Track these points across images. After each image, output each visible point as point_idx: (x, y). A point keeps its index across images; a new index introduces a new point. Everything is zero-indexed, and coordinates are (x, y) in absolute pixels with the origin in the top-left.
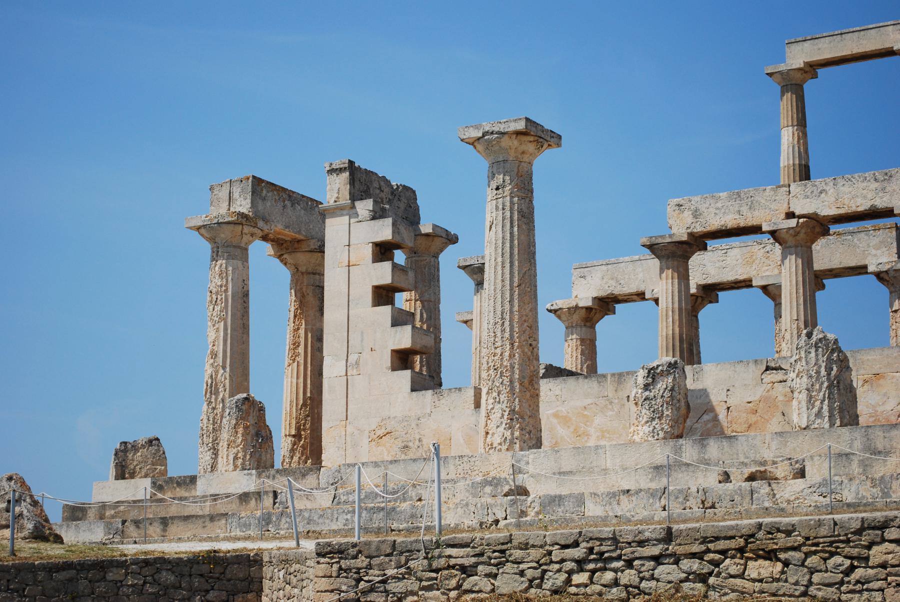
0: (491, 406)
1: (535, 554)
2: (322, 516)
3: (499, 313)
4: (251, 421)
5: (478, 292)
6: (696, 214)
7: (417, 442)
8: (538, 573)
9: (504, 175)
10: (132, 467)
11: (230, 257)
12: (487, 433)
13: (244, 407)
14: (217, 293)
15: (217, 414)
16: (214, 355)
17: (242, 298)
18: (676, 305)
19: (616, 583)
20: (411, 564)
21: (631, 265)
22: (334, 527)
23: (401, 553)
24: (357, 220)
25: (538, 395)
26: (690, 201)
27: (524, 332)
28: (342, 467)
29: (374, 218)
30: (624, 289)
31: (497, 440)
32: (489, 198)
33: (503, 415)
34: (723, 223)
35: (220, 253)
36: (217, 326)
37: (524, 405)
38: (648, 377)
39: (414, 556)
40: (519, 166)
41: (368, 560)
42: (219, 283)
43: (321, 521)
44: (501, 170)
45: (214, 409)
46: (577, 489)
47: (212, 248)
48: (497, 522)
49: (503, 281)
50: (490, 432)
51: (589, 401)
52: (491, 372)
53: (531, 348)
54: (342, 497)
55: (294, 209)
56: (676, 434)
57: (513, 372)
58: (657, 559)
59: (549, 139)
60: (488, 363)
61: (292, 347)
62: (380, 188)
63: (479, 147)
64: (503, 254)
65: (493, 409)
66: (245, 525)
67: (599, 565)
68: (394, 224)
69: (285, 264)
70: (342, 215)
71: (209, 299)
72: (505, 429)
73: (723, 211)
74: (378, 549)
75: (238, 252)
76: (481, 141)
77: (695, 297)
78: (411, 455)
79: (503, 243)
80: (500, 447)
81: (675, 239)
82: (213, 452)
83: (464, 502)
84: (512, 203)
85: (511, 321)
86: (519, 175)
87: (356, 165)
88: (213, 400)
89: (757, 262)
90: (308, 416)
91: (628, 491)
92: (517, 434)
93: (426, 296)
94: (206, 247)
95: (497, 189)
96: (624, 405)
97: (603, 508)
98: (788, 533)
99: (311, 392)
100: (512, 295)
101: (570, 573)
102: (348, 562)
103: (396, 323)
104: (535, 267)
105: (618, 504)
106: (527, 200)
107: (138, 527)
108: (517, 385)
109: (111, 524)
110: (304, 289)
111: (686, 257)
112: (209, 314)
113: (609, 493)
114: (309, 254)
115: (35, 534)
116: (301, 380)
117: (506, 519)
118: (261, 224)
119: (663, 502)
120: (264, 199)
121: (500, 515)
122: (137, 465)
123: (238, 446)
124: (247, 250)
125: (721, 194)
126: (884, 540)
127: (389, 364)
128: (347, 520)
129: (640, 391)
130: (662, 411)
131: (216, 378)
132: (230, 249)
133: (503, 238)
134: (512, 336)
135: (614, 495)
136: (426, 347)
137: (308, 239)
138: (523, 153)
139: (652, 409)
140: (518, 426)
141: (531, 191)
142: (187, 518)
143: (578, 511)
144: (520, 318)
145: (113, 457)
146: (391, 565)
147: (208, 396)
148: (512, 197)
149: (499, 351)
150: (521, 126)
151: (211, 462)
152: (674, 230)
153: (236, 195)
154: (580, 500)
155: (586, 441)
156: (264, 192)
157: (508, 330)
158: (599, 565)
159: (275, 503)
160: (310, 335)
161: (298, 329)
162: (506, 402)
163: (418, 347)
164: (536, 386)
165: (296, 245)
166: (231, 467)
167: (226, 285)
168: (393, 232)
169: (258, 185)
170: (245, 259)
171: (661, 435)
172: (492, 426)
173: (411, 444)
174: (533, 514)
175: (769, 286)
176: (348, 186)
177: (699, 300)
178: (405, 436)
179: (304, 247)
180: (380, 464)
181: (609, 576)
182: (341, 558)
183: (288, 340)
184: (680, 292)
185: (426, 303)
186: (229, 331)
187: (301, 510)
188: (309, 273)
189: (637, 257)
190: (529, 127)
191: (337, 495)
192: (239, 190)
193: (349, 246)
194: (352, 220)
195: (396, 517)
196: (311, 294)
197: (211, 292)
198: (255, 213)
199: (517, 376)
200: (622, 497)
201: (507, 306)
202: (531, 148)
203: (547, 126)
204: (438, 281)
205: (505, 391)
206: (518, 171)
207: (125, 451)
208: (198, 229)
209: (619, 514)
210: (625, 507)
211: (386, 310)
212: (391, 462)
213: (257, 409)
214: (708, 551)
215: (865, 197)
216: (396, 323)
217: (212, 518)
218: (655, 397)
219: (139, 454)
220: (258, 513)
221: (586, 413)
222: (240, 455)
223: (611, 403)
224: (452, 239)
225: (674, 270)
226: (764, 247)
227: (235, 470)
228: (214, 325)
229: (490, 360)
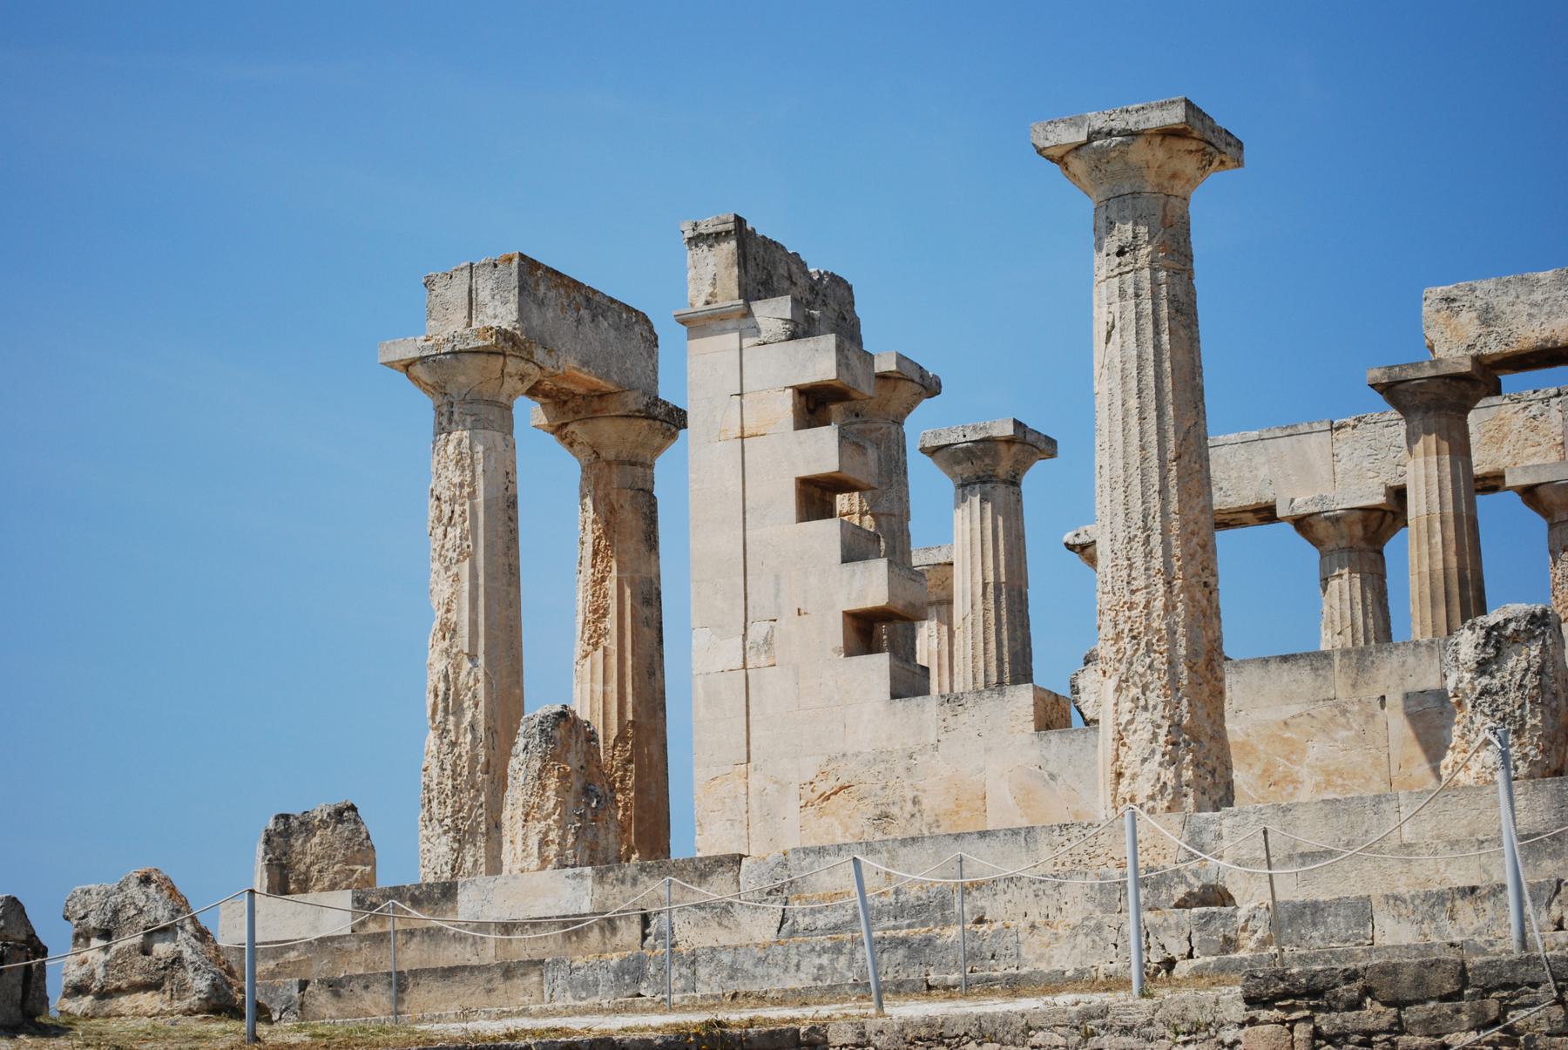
0: (1128, 717)
2: (760, 961)
3: (1137, 517)
4: (573, 762)
5: (964, 501)
6: (1487, 317)
7: (909, 807)
9: (1136, 224)
10: (302, 868)
11: (478, 424)
12: (1119, 775)
13: (557, 734)
14: (453, 500)
15: (460, 756)
16: (449, 630)
17: (505, 508)
18: (1449, 510)
20: (1517, 1018)
21: (1242, 451)
22: (792, 983)
23: (1486, 991)
24: (756, 340)
25: (1222, 693)
26: (1473, 290)
27: (1193, 556)
28: (791, 856)
29: (793, 336)
30: (1229, 500)
31: (1144, 789)
32: (1103, 274)
33: (1155, 736)
34: (1547, 334)
35: (456, 416)
36: (454, 569)
37: (1199, 712)
38: (1485, 645)
39: (1525, 999)
40: (1165, 205)
41: (1393, 1010)
42: (457, 480)
43: (760, 971)
44: (1127, 213)
45: (453, 744)
46: (1352, 888)
47: (437, 408)
48: (1170, 964)
49: (1143, 448)
50: (1128, 773)
51: (1294, 709)
52: (1126, 644)
53: (1207, 591)
54: (800, 918)
55: (597, 326)
56: (1554, 766)
57: (1174, 644)
59: (1223, 147)
60: (1116, 625)
61: (590, 616)
62: (790, 277)
63: (1077, 165)
64: (1140, 391)
65: (1131, 722)
66: (585, 985)
69: (571, 445)
70: (724, 331)
71: (432, 514)
72: (1161, 764)
73: (1546, 309)
74: (1419, 981)
75: (494, 414)
76: (1082, 152)
77: (1378, 514)
78: (897, 833)
79: (1140, 369)
80: (1151, 803)
81: (1445, 370)
82: (454, 838)
83: (1092, 923)
84: (1155, 283)
85: (1165, 533)
86: (1167, 224)
87: (749, 227)
88: (451, 727)
89: (1513, 437)
90: (629, 761)
91: (1473, 889)
92: (1188, 774)
93: (884, 505)
94: (423, 406)
95: (1121, 253)
96: (1373, 716)
97: (1415, 927)
99: (635, 711)
100: (1163, 479)
102: (1337, 1018)
103: (852, 554)
104: (1204, 418)
105: (1452, 918)
106: (1185, 277)
107: (337, 995)
108: (1183, 670)
109: (275, 989)
110: (613, 497)
112: (436, 545)
113: (1428, 896)
114: (623, 424)
115: (214, 1001)
116: (613, 685)
117: (1190, 956)
118: (539, 354)
119: (1556, 911)
120: (541, 304)
121: (1176, 948)
122: (312, 864)
123: (549, 816)
124: (509, 408)
125: (1541, 275)
127: (840, 642)
128: (821, 967)
129: (1468, 676)
130: (1522, 717)
131: (456, 679)
132: (476, 408)
133: (1139, 356)
134: (1167, 564)
135: (1441, 898)
136: (913, 605)
137: (623, 390)
138: (1174, 176)
139: (1499, 715)
140: (1189, 758)
141: (1189, 257)
142: (449, 973)
143: (1357, 936)
144: (1183, 527)
145: (263, 846)
146: (1460, 1023)
147: (439, 718)
148: (1154, 271)
149: (1140, 598)
150: (1175, 116)
151: (451, 857)
152: (1440, 352)
153: (484, 295)
154: (1362, 911)
155: (1291, 795)
156: (542, 288)
157: (1159, 552)
159: (645, 937)
160: (628, 592)
161: (603, 579)
162: (1160, 707)
163: (899, 606)
164: (1219, 674)
165: (596, 404)
166: (535, 862)
167: (472, 484)
168: (839, 365)
169: (531, 274)
170: (507, 427)
171: (1523, 768)
172: (1130, 759)
173: (895, 810)
174: (1252, 944)
175: (1540, 488)
176: (736, 270)
177: (1389, 518)
178: (880, 793)
179: (614, 407)
180: (877, 846)
182: (1316, 1009)
183: (580, 605)
184: (1455, 480)
185: (883, 519)
186: (481, 580)
187: (713, 949)
188: (623, 463)
189: (1254, 434)
190: (1191, 120)
191: (788, 914)
192: (491, 284)
193: (741, 395)
194: (747, 342)
195: (934, 959)
196: (627, 506)
197: (438, 499)
198: (526, 331)
199: (1182, 652)
200: (1459, 903)
201: (1155, 503)
202: (1190, 165)
203: (1220, 122)
204: (905, 472)
205: (1159, 684)
206: (1165, 216)
207: (287, 833)
208: (407, 366)
209: (1457, 939)
210: (1467, 925)
212: (904, 842)
213: (582, 737)
216: (852, 554)
217: (508, 971)
218: (1503, 687)
219: (316, 840)
220: (615, 959)
221: (1288, 735)
222: (552, 836)
223: (1344, 712)
224: (931, 387)
225: (1440, 437)
226: (1526, 408)
227: (543, 868)
228: (447, 569)
229: (1121, 619)
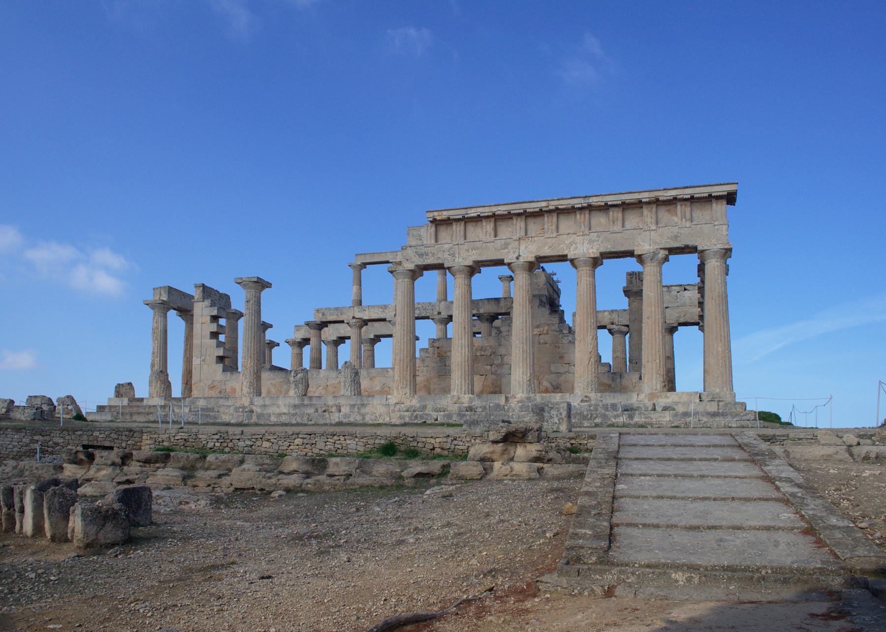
1: (205, 437)
6: (323, 314)
8: (206, 442)
19: (227, 446)
29: (211, 306)
58: (239, 439)
67: (223, 440)
68: (218, 309)
98: (274, 434)
101: (215, 442)
111: (320, 330)
126: (298, 438)
158: (223, 440)
181: (225, 445)
211: (214, 341)
214: (252, 438)
215: (378, 314)
216: (217, 346)
